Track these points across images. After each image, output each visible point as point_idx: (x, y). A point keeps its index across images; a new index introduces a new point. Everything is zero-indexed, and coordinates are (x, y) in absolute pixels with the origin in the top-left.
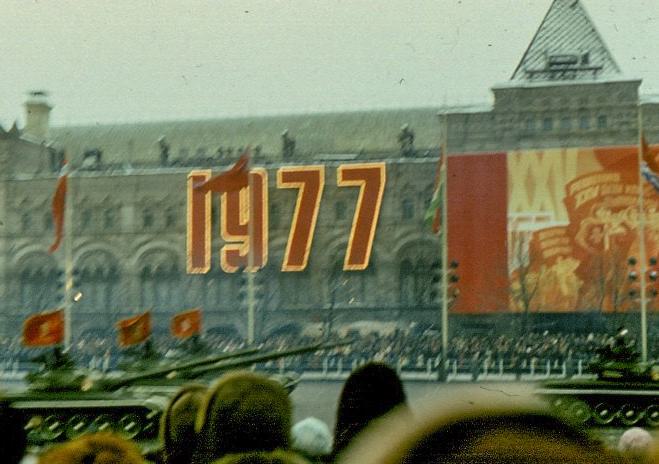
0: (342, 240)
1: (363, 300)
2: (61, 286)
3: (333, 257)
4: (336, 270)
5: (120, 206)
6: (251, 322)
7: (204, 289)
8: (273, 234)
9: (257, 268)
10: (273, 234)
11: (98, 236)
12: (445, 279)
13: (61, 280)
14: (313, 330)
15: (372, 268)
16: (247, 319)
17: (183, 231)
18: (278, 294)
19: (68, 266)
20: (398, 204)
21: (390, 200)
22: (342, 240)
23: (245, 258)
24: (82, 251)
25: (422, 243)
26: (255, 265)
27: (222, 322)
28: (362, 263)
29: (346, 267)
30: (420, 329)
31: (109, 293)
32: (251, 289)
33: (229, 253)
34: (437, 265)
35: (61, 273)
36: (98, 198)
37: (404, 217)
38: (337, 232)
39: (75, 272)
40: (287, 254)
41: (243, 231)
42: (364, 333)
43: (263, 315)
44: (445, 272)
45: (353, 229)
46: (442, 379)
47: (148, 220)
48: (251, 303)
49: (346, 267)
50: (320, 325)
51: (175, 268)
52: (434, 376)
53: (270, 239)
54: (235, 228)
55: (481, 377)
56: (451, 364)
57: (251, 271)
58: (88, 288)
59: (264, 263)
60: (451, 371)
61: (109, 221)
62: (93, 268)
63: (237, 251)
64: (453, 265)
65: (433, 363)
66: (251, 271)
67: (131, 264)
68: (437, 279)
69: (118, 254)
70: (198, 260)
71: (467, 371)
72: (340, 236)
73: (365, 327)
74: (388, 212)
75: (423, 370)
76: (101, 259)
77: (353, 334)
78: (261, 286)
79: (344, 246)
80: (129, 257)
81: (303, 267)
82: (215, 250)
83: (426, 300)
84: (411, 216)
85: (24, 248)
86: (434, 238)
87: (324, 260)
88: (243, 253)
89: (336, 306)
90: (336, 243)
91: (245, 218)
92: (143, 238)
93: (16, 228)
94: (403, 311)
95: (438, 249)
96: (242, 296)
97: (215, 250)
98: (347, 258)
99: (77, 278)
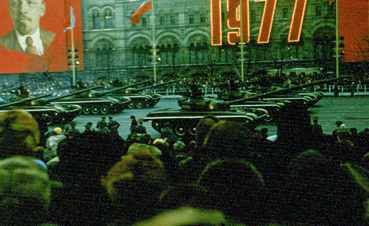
0: (288, 27)
1: (297, 58)
2: (151, 54)
3: (282, 36)
4: (284, 42)
5: (178, 14)
6: (242, 69)
7: (220, 53)
8: (252, 25)
9: (245, 43)
10: (252, 25)
11: (168, 29)
12: (337, 45)
13: (151, 50)
14: (273, 72)
15: (302, 42)
16: (240, 68)
17: (209, 25)
18: (255, 56)
19: (154, 44)
20: (314, 7)
21: (309, 6)
22: (288, 27)
23: (239, 37)
24: (160, 37)
25: (327, 27)
26: (244, 42)
27: (227, 69)
28: (297, 39)
29: (289, 41)
30: (323, 71)
31: (174, 57)
32: (242, 53)
33: (230, 35)
34: (334, 38)
35: (151, 48)
36: (167, 10)
37: (317, 15)
38: (284, 23)
39: (158, 47)
40: (260, 35)
41: (237, 24)
42: (297, 74)
43: (249, 65)
44: (337, 42)
45: (292, 21)
46: (336, 96)
47: (191, 20)
48: (242, 60)
49: (289, 41)
50: (277, 70)
51: (205, 43)
52: (332, 94)
53: (251, 28)
54: (234, 23)
55: (355, 94)
56: (340, 88)
57: (242, 44)
58: (164, 54)
59: (249, 39)
60: (341, 91)
61: (173, 22)
62: (166, 45)
63: (236, 34)
64: (342, 38)
65: (332, 87)
66: (242, 44)
67: (184, 42)
68: (334, 45)
69: (178, 38)
70: (216, 40)
71: (349, 91)
72: (286, 25)
73: (298, 70)
74: (309, 13)
75: (327, 91)
76: (170, 40)
77: (293, 74)
78: (246, 52)
79: (288, 30)
80: (183, 39)
81: (268, 42)
82: (224, 34)
83: (328, 55)
84: (320, 14)
85: (133, 36)
86: (332, 25)
87: (278, 37)
88: (238, 35)
89: (284, 60)
90: (283, 30)
91: (238, 18)
92: (190, 29)
93: (129, 26)
94: (317, 62)
95: (334, 30)
96: (238, 57)
97: (224, 34)
98: (289, 36)
99: (158, 50)
